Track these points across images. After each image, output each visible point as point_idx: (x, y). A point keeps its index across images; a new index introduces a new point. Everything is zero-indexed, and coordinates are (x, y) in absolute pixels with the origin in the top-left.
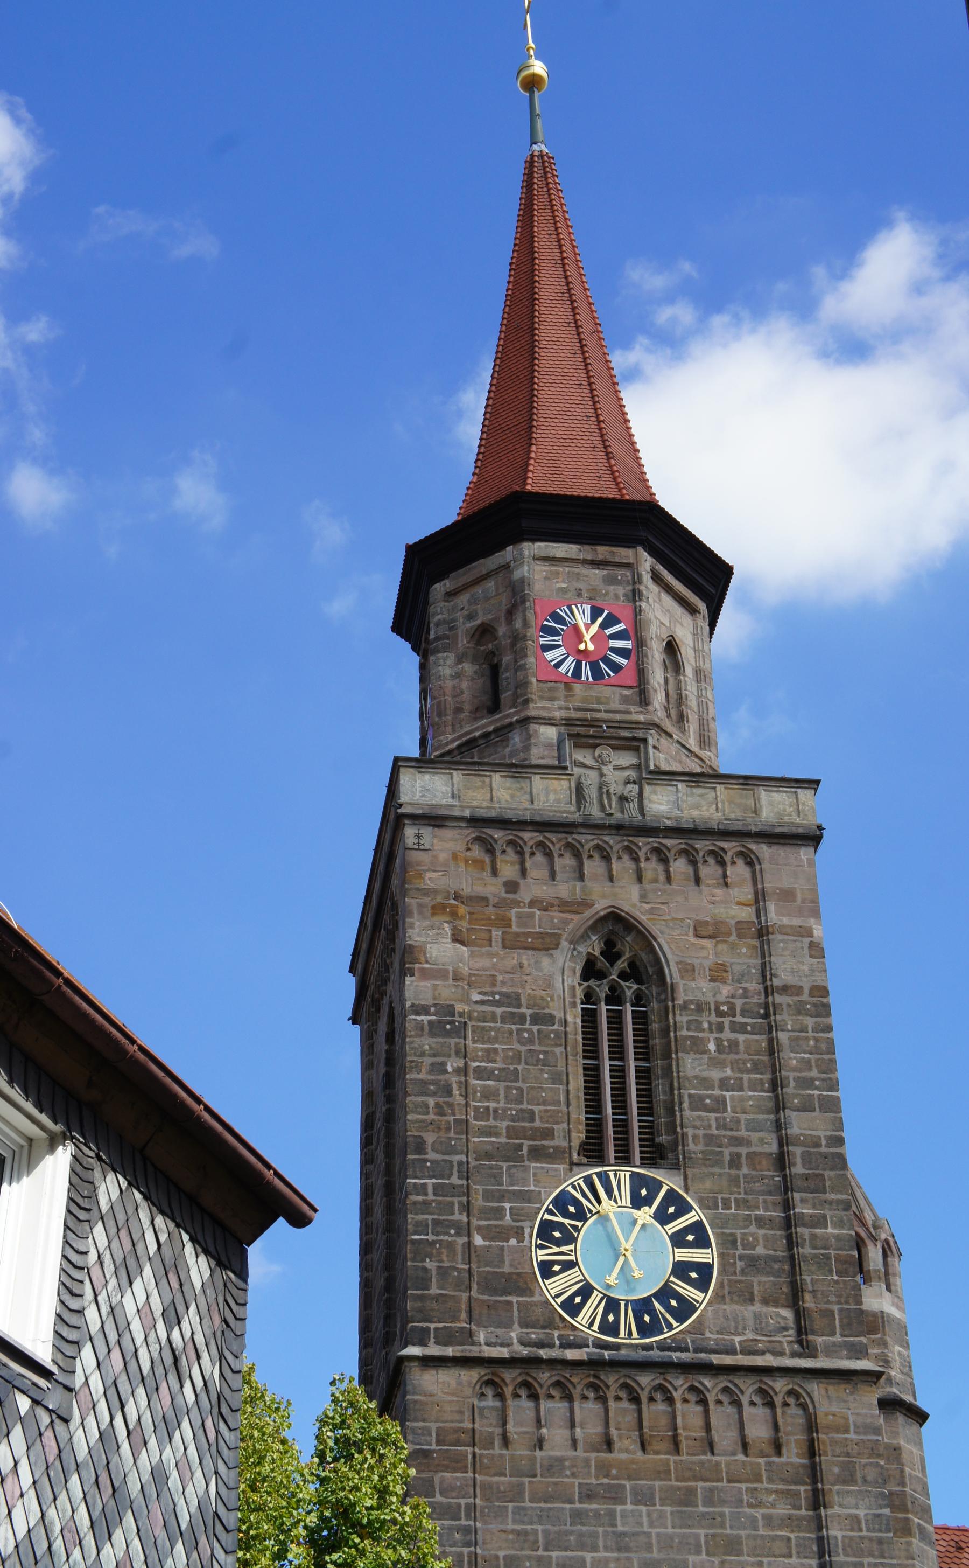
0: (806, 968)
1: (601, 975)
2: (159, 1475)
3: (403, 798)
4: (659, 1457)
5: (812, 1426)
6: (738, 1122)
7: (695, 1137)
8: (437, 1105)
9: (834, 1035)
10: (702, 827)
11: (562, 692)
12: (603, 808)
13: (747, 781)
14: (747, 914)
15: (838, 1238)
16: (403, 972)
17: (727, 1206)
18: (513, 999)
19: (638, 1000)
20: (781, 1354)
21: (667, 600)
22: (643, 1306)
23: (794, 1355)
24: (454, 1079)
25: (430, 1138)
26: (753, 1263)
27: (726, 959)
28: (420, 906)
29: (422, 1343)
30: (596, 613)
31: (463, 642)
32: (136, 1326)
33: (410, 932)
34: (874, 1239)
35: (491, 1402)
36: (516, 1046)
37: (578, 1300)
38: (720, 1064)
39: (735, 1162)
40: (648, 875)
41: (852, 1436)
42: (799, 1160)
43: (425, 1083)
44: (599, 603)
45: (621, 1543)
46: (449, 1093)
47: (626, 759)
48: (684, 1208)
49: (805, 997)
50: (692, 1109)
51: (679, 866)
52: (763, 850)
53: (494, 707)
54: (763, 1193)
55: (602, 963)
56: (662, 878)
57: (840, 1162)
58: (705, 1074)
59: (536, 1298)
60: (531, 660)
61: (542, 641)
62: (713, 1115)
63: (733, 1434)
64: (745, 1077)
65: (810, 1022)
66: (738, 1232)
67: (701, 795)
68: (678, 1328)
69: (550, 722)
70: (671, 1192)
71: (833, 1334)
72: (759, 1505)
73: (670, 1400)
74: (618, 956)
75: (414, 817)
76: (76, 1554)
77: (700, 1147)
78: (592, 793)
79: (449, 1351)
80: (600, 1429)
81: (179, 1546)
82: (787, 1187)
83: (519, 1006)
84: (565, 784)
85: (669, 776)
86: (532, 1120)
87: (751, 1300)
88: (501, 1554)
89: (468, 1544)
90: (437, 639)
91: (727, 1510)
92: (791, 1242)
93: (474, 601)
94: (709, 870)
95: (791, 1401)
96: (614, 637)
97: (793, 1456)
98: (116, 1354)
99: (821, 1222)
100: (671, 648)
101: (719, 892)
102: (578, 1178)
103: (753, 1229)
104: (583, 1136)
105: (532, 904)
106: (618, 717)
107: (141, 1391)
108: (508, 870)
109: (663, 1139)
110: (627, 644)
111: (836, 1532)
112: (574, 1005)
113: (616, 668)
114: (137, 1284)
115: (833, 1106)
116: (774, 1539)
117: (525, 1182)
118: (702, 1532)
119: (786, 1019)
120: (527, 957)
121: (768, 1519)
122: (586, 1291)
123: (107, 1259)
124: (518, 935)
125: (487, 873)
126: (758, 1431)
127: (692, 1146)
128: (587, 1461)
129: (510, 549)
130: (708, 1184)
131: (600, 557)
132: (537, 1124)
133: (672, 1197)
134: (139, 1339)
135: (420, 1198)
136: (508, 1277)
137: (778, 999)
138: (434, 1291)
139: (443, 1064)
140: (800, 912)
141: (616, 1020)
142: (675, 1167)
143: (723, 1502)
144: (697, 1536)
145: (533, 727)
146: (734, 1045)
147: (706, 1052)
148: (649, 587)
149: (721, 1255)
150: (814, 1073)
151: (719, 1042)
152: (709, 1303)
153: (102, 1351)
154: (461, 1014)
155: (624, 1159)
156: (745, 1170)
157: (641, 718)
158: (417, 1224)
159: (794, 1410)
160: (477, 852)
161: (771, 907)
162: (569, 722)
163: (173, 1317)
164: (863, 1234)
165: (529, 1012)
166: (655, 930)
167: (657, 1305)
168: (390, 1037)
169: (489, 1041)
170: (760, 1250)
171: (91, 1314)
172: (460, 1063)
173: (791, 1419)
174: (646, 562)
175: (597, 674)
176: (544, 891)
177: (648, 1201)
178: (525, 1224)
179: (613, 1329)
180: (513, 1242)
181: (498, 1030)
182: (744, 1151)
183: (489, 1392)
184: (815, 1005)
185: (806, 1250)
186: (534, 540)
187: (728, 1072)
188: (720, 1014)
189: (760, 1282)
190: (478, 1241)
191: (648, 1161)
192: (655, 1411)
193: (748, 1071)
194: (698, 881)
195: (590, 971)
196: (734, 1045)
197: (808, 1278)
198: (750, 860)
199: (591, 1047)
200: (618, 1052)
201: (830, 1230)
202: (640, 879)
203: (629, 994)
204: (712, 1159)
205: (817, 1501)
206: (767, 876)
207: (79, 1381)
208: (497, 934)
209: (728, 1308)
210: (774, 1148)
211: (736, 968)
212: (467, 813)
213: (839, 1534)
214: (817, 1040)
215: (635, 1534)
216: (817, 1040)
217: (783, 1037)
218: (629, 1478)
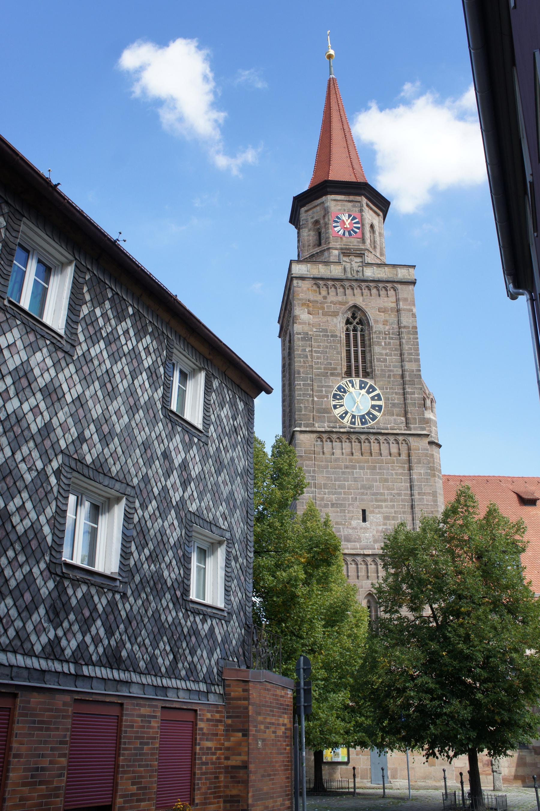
0: (411, 321)
2: (232, 459)
3: (293, 272)
4: (367, 457)
5: (409, 449)
6: (390, 365)
7: (378, 370)
9: (419, 340)
10: (381, 280)
11: (339, 240)
12: (352, 274)
13: (394, 266)
14: (394, 305)
15: (418, 398)
16: (293, 323)
17: (387, 389)
18: (325, 331)
19: (362, 330)
20: (401, 430)
21: (371, 212)
22: (362, 417)
23: (405, 430)
24: (308, 354)
25: (302, 370)
26: (394, 405)
27: (388, 318)
28: (298, 304)
29: (300, 427)
30: (350, 216)
31: (310, 225)
32: (225, 420)
33: (295, 311)
34: (428, 398)
35: (319, 443)
36: (326, 344)
37: (344, 415)
38: (386, 349)
39: (389, 377)
40: (365, 294)
41: (420, 451)
42: (408, 376)
43: (300, 354)
44: (350, 213)
45: (355, 480)
46: (307, 357)
47: (359, 260)
48: (374, 390)
49: (410, 329)
50: (377, 362)
51: (374, 291)
52: (399, 286)
53: (320, 244)
54: (397, 385)
55: (351, 320)
56: (369, 295)
57: (420, 376)
58: (381, 352)
59: (332, 415)
60: (330, 230)
61: (334, 225)
62: (383, 363)
63: (387, 451)
64: (393, 352)
65: (412, 336)
69: (336, 249)
70: (371, 385)
71: (416, 424)
72: (394, 470)
73: (370, 442)
74: (356, 318)
76: (212, 478)
77: (379, 373)
78: (348, 270)
79: (308, 429)
80: (350, 450)
81: (238, 478)
82: (404, 384)
83: (327, 332)
84: (341, 267)
85: (371, 265)
86: (331, 365)
87: (393, 415)
88: (322, 482)
89: (313, 480)
90: (303, 224)
91: (385, 471)
92: (405, 399)
94: (383, 292)
95: (404, 442)
96: (355, 223)
97: (404, 457)
98: (219, 428)
99: (413, 393)
100: (372, 226)
101: (386, 299)
102: (344, 381)
103: (394, 395)
104: (346, 370)
105: (331, 303)
106: (356, 247)
107: (226, 438)
108: (324, 292)
109: (369, 370)
110: (359, 225)
111: (415, 477)
112: (343, 332)
113: (355, 232)
114: (224, 409)
115: (418, 360)
116: (397, 478)
117: (329, 383)
118: (378, 477)
119: (405, 336)
120: (329, 318)
121: (396, 474)
122: (346, 413)
123: (216, 402)
124: (327, 312)
126: (394, 450)
127: (377, 372)
128: (346, 459)
129: (324, 197)
131: (351, 199)
132: (332, 366)
133: (371, 387)
134: (226, 424)
135: (299, 387)
136: (324, 409)
137: (403, 330)
138: (303, 413)
139: (305, 349)
140: (409, 305)
141: (355, 336)
142: (372, 378)
143: (384, 469)
144: (376, 478)
145: (331, 250)
146: (389, 343)
147: (382, 345)
149: (385, 403)
150: (413, 351)
151: (385, 343)
152: (381, 416)
153: (216, 427)
154: (310, 335)
155: (357, 376)
156: (392, 379)
157: (363, 247)
158: (298, 394)
159: (404, 445)
160: (315, 287)
161: (401, 303)
162: (342, 249)
163: (234, 418)
164: (425, 397)
165: (330, 334)
166: (367, 310)
167: (366, 416)
168: (290, 341)
169: (318, 342)
170: (396, 401)
171: (212, 417)
172: (310, 349)
173: (403, 448)
174: (364, 200)
175: (350, 234)
177: (364, 388)
178: (329, 394)
179: (354, 423)
180: (325, 399)
181: (321, 339)
182: (392, 373)
183: (319, 440)
184: (413, 332)
185: (409, 401)
186: (331, 195)
189: (396, 410)
190: (316, 399)
192: (365, 446)
193: (393, 351)
194: (379, 295)
195: (348, 322)
196: (389, 343)
197: (409, 409)
198: (395, 290)
199: (348, 344)
200: (356, 346)
202: (362, 295)
203: (359, 329)
204: (383, 376)
205: (410, 469)
206: (400, 294)
207: (210, 434)
208: (320, 311)
209: (386, 417)
210: (401, 373)
211: (391, 321)
212: (312, 276)
213: (416, 477)
214: (413, 342)
215: (359, 477)
216: (413, 342)
217: (404, 341)
218: (358, 463)
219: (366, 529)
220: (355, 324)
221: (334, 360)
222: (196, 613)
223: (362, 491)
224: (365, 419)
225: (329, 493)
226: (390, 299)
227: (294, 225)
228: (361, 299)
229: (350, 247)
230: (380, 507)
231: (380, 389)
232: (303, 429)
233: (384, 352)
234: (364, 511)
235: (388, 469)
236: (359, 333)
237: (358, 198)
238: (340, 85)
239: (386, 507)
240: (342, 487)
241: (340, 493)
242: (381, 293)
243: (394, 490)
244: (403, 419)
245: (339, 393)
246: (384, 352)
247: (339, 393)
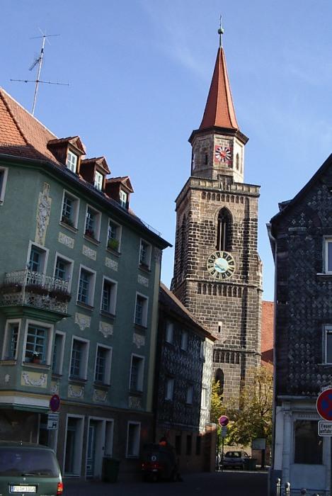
18: (207, 221)
52: (250, 198)
69: (216, 170)
75: (193, 189)
79: (193, 279)
100: (237, 155)
122: (215, 271)
142: (229, 251)
148: (235, 144)
155: (222, 250)
174: (235, 139)
191: (226, 250)
232: (191, 279)
237: (231, 138)
238: (224, 52)
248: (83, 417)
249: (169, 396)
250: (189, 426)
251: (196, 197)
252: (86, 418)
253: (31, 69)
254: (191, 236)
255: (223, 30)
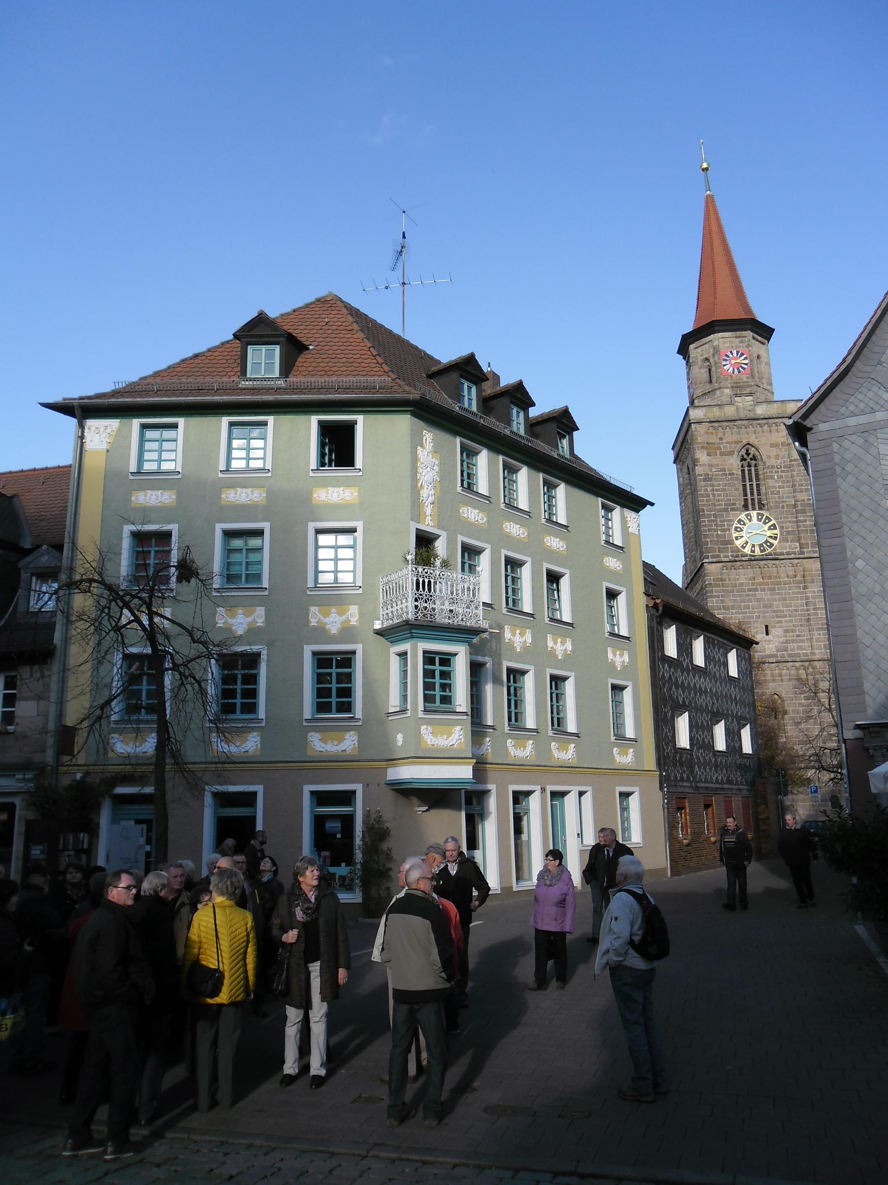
1: (745, 460)
7: (772, 502)
8: (707, 500)
11: (730, 378)
15: (810, 524)
16: (695, 465)
21: (757, 343)
22: (761, 545)
23: (799, 554)
24: (710, 493)
25: (705, 508)
26: (788, 532)
27: (779, 453)
30: (738, 352)
31: (700, 363)
39: (783, 507)
40: (757, 432)
41: (813, 572)
44: (738, 350)
45: (758, 600)
46: (709, 496)
48: (770, 520)
55: (745, 456)
56: (761, 432)
61: (723, 363)
66: (784, 525)
67: (770, 408)
68: (770, 550)
74: (750, 454)
77: (774, 504)
78: (741, 410)
79: (715, 560)
87: (788, 542)
90: (692, 362)
93: (702, 350)
99: (806, 521)
101: (776, 434)
105: (727, 443)
113: (744, 369)
122: (747, 543)
125: (714, 436)
127: (772, 504)
129: (712, 335)
130: (776, 514)
132: (732, 502)
138: (709, 546)
139: (707, 489)
141: (750, 471)
143: (782, 590)
145: (722, 390)
146: (782, 476)
147: (774, 479)
149: (780, 531)
151: (778, 476)
155: (754, 509)
156: (785, 509)
162: (732, 387)
166: (759, 446)
167: (764, 545)
170: (790, 529)
175: (739, 372)
176: (729, 440)
182: (785, 504)
187: (780, 484)
188: (778, 468)
189: (790, 537)
190: (719, 533)
191: (760, 509)
194: (770, 432)
195: (743, 459)
196: (782, 476)
200: (751, 480)
201: (808, 523)
204: (777, 507)
208: (718, 452)
212: (708, 421)
219: (769, 641)
220: (749, 460)
221: (733, 496)
222: (745, 758)
223: (765, 609)
224: (763, 547)
225: (736, 613)
226: (780, 434)
227: (682, 355)
228: (753, 437)
229: (739, 384)
230: (781, 622)
231: (775, 519)
232: (710, 560)
233: (777, 485)
234: (767, 627)
235: (786, 590)
236: (753, 468)
239: (786, 622)
240: (747, 607)
241: (746, 613)
242: (772, 428)
243: (791, 607)
244: (798, 544)
245: (739, 526)
246: (777, 485)
247: (739, 526)
248: (538, 788)
249: (683, 740)
250: (725, 786)
251: (700, 433)
252: (543, 790)
253: (393, 269)
254: (702, 495)
255: (705, 165)
